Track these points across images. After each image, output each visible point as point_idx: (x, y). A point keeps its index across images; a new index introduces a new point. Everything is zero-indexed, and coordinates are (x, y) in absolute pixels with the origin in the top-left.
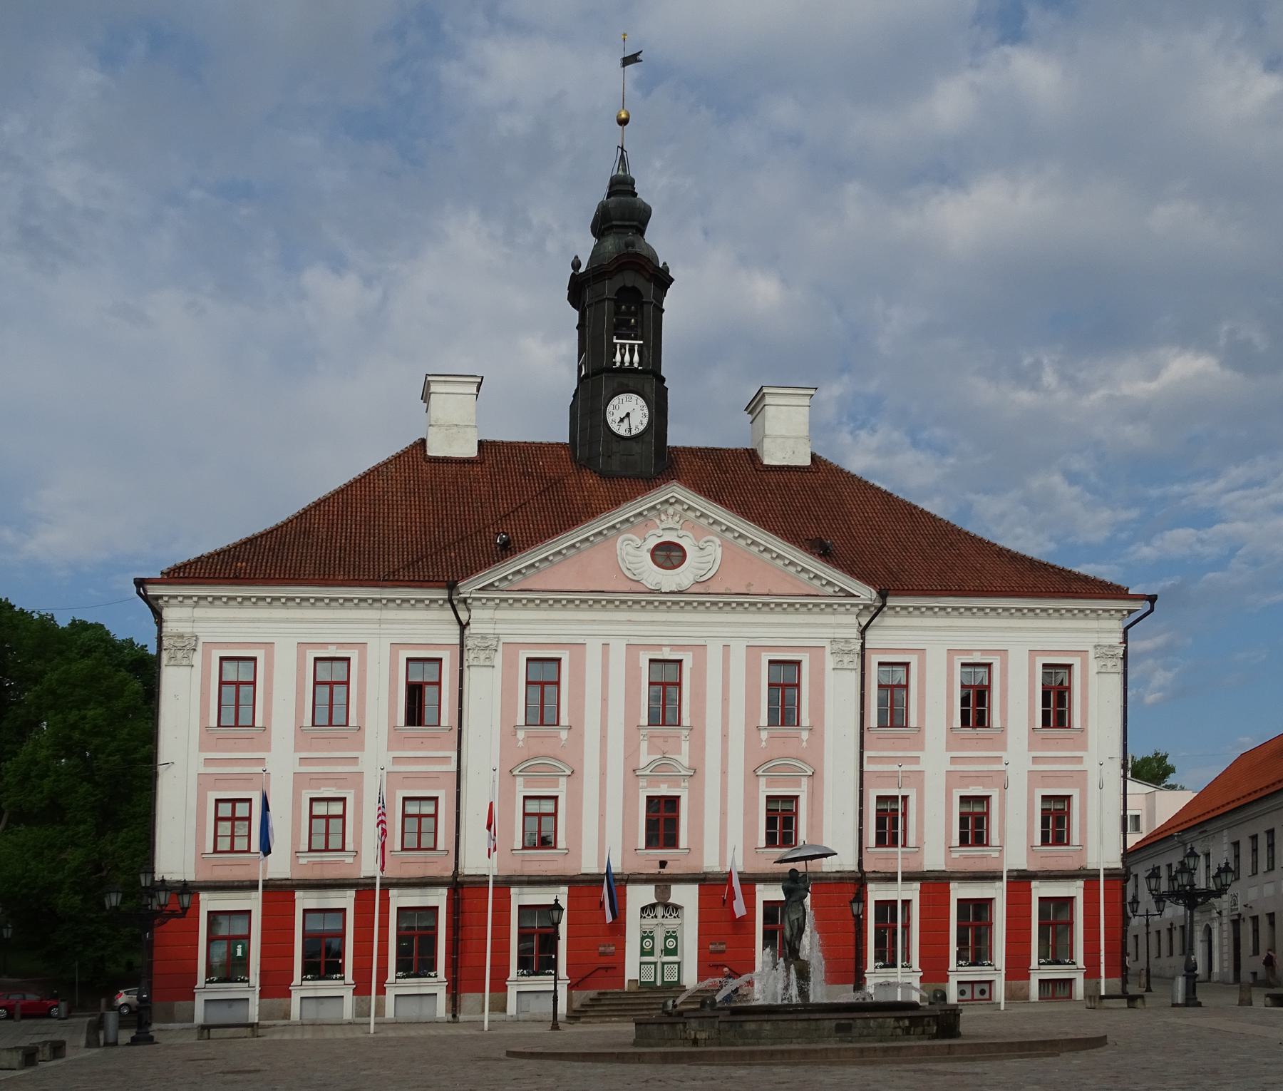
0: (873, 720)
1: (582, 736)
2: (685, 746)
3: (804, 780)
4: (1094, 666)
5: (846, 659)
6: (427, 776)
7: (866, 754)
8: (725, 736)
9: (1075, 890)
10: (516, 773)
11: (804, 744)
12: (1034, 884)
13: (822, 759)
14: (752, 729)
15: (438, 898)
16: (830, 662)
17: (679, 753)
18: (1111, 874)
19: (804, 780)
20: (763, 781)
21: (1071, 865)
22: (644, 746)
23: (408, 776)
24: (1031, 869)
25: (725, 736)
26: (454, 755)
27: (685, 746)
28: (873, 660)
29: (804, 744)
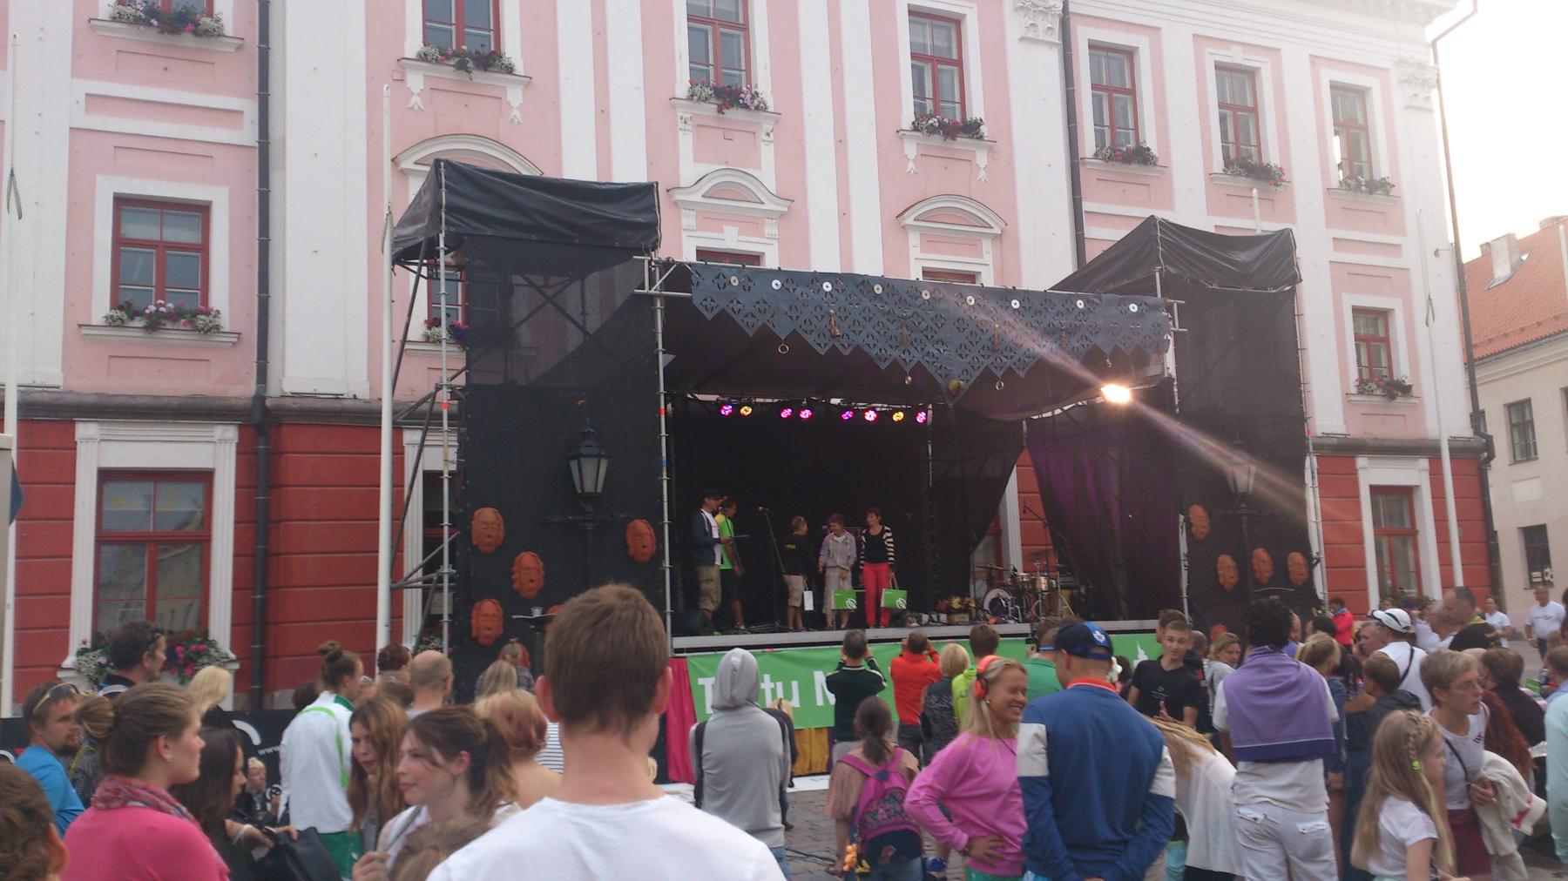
0: (1088, 146)
1: (556, 103)
2: (767, 153)
3: (987, 246)
4: (1399, 98)
5: (1043, 24)
6: (178, 150)
7: (1087, 206)
8: (841, 142)
9: (1413, 473)
10: (407, 164)
11: (982, 174)
12: (1361, 462)
13: (1013, 208)
14: (890, 138)
15: (215, 451)
16: (1014, 26)
17: (759, 167)
18: (1460, 451)
19: (987, 246)
20: (914, 239)
21: (1394, 429)
22: (686, 142)
23: (127, 145)
24: (1357, 432)
25: (841, 142)
26: (251, 108)
27: (767, 153)
28: (1083, 36)
29: (982, 174)
